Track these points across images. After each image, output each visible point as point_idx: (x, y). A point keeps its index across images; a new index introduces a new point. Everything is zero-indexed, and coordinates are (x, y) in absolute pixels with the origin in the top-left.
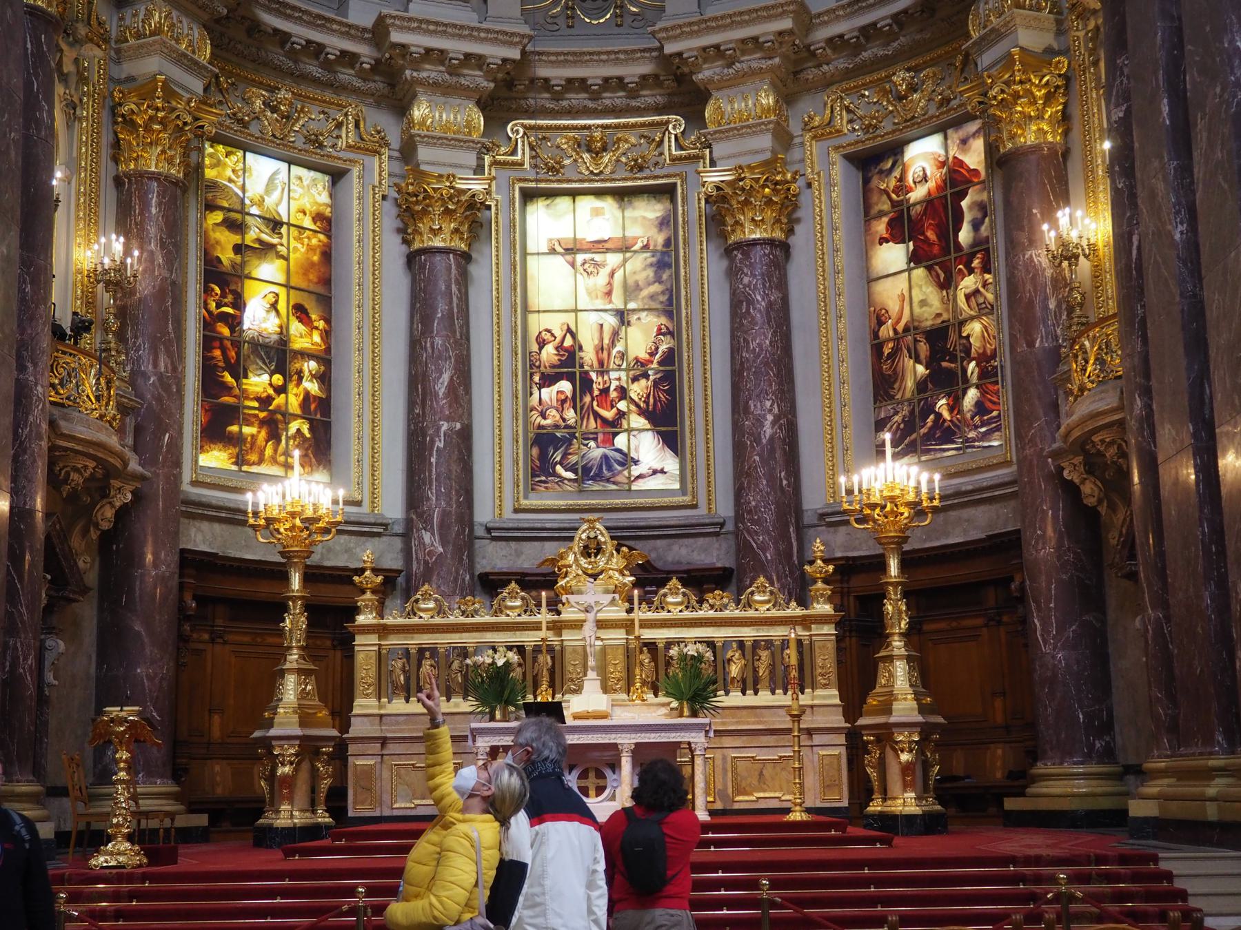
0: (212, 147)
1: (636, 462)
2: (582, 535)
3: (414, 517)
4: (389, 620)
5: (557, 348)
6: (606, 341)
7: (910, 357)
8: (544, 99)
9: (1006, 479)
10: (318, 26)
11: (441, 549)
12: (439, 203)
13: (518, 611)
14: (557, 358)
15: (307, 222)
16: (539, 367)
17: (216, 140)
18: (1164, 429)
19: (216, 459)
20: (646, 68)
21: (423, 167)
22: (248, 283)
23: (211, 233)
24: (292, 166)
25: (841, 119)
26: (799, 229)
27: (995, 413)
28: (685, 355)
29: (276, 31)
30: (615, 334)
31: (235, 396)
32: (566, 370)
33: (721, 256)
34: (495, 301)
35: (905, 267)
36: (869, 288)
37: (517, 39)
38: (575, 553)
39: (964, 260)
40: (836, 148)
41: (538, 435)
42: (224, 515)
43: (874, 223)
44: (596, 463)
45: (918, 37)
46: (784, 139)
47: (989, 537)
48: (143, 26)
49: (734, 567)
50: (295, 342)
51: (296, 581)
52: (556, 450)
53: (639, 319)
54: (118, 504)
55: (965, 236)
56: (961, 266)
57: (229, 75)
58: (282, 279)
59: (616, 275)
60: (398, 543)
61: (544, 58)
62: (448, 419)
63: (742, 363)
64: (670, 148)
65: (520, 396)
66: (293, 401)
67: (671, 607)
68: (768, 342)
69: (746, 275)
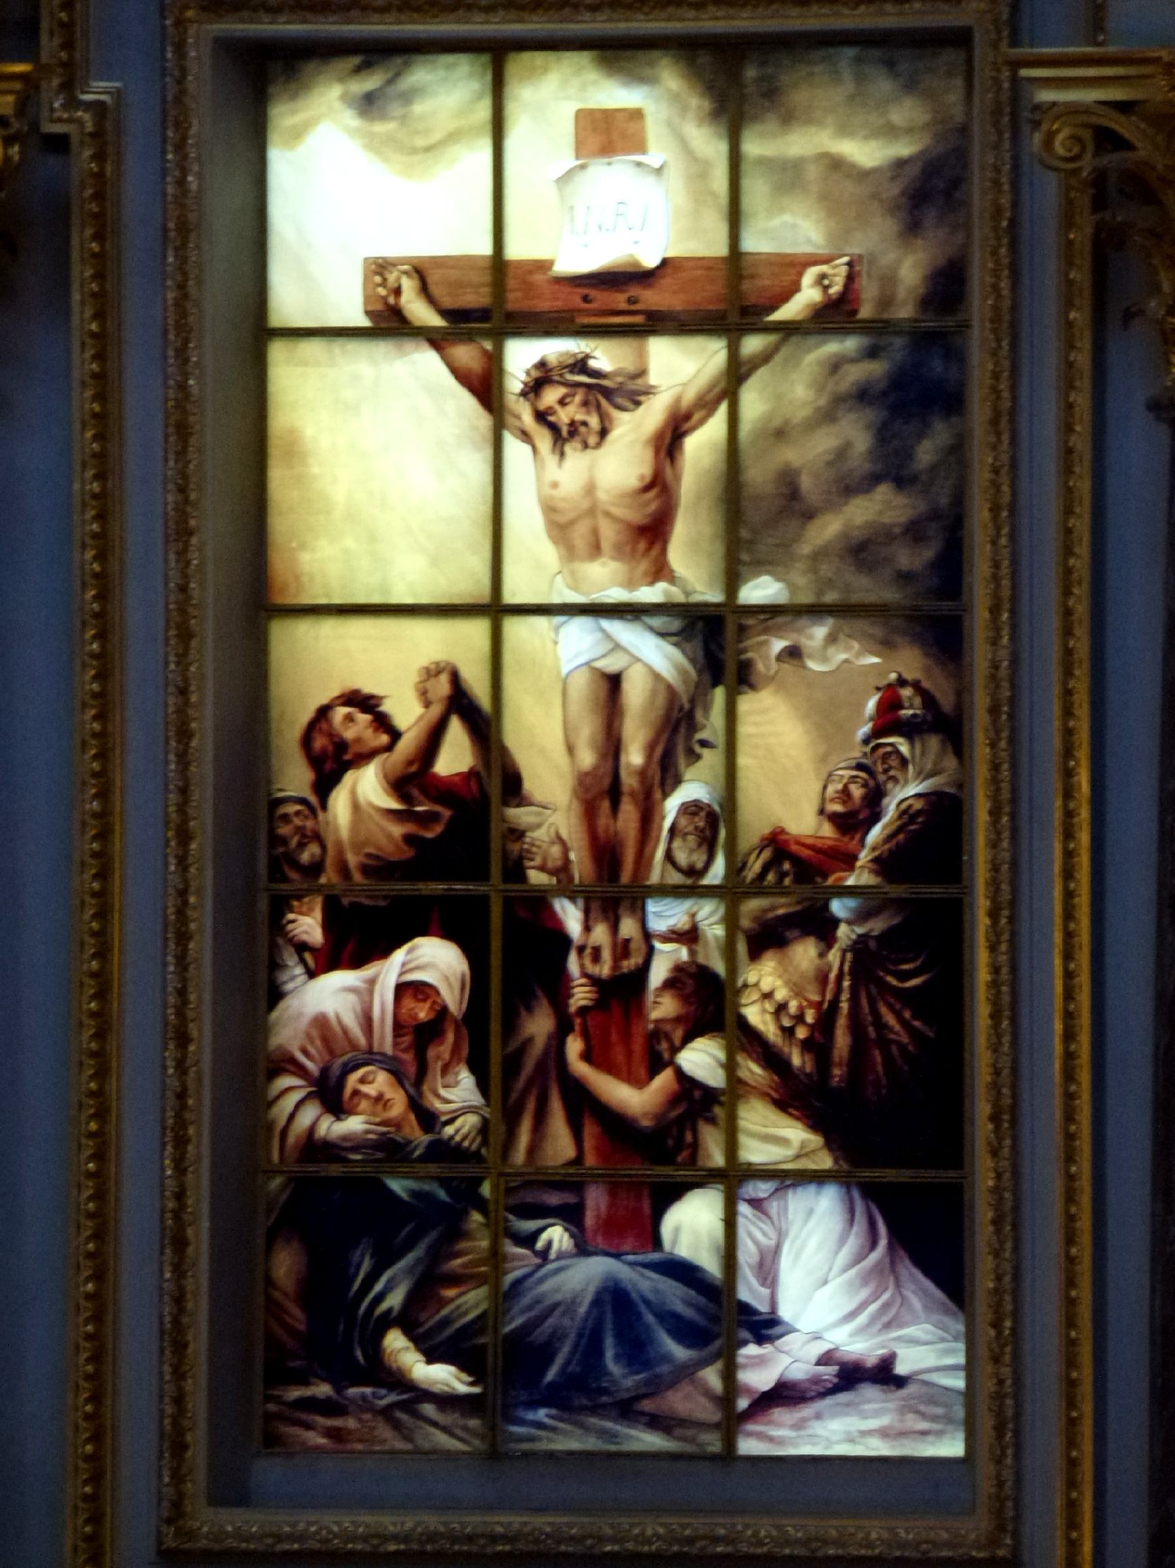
5: (399, 785)
6: (634, 756)
14: (397, 830)
16: (316, 868)
32: (439, 887)
41: (300, 1185)
44: (571, 1325)
53: (793, 653)
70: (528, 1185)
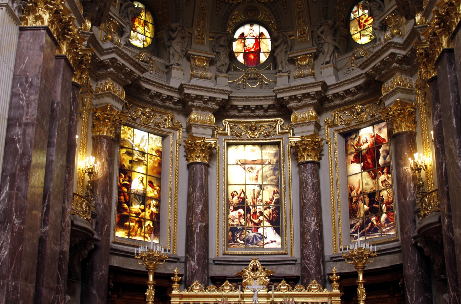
0: (123, 127)
1: (266, 238)
2: (251, 264)
3: (188, 256)
4: (183, 293)
5: (238, 198)
6: (256, 195)
7: (362, 203)
8: (235, 113)
9: (397, 246)
10: (160, 87)
11: (197, 268)
12: (199, 147)
13: (228, 291)
14: (238, 201)
15: (154, 153)
16: (232, 204)
17: (125, 125)
18: (456, 230)
19: (121, 234)
20: (271, 103)
21: (194, 135)
22: (134, 173)
23: (122, 156)
24: (150, 134)
25: (338, 121)
26: (323, 158)
27: (392, 223)
28: (283, 201)
29: (146, 89)
30: (259, 193)
31: (128, 212)
33: (296, 167)
34: (217, 181)
35: (360, 171)
36: (347, 179)
37: (227, 92)
38: (249, 271)
39: (381, 169)
40: (336, 131)
41: (231, 228)
42: (123, 254)
43: (349, 156)
44: (251, 238)
45: (364, 94)
46: (318, 127)
47: (391, 266)
48: (104, 88)
49: (300, 275)
50: (148, 194)
51: (151, 278)
52: (237, 233)
53: (267, 188)
54: (90, 249)
55: (381, 161)
56: (380, 172)
57: (130, 103)
58: (145, 172)
59: (259, 173)
60: (183, 265)
61: (236, 99)
62: (201, 222)
63: (304, 204)
64: (279, 129)
65: (225, 214)
66: (147, 215)
67: (282, 290)
68: (313, 197)
69: (305, 173)
70: (248, 228)
